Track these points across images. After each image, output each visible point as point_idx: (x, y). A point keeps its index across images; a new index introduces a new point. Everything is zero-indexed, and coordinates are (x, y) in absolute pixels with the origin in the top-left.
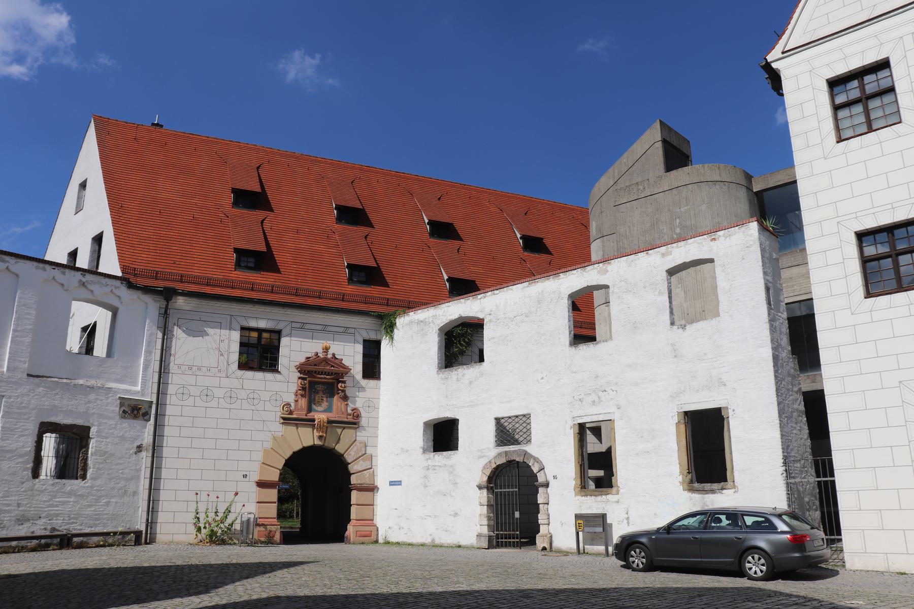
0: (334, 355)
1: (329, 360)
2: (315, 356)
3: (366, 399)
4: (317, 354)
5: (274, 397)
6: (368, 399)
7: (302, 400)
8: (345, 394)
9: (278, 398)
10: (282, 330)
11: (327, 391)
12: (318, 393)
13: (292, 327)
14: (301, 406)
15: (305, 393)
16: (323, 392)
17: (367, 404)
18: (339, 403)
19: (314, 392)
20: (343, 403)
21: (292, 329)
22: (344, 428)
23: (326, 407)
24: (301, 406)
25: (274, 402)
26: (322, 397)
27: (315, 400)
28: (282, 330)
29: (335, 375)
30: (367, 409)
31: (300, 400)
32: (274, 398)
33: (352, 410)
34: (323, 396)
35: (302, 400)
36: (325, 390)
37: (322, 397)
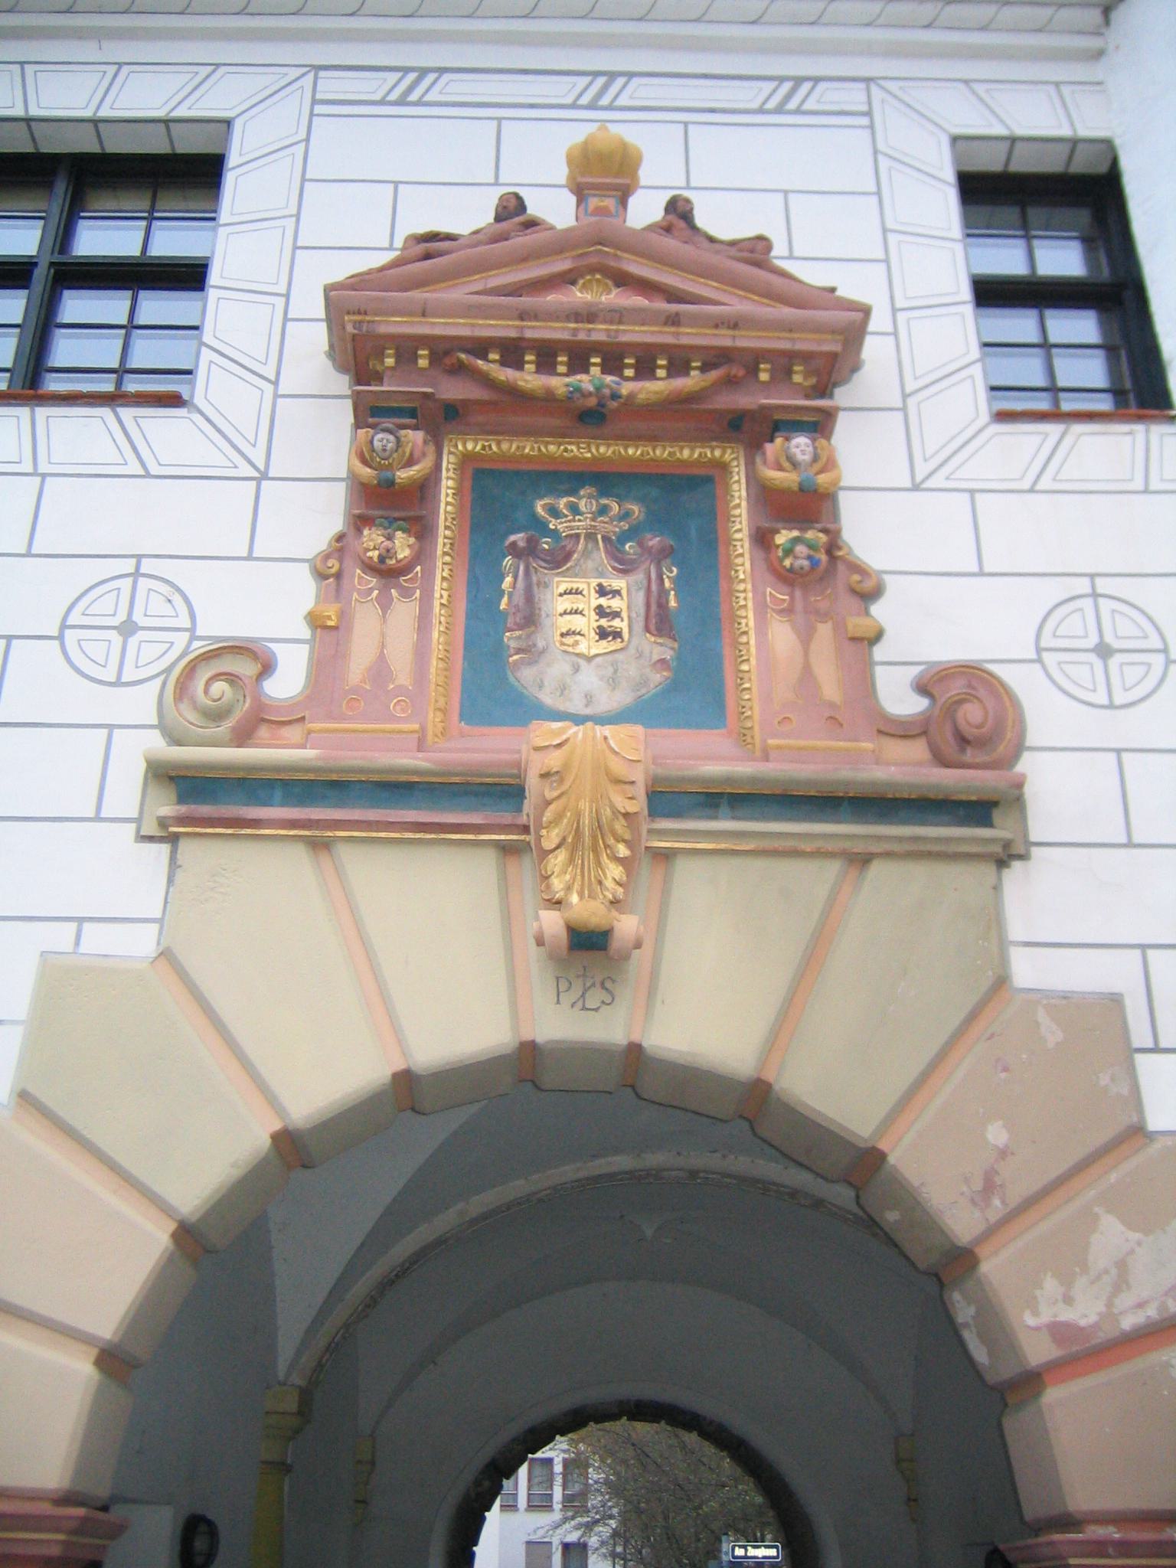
0: (679, 211)
1: (635, 245)
2: (498, 219)
3: (1057, 590)
4: (512, 209)
5: (106, 605)
6: (1083, 586)
7: (385, 604)
8: (833, 546)
9: (152, 607)
10: (228, 123)
11: (654, 542)
12: (559, 560)
13: (315, 102)
14: (380, 670)
15: (422, 555)
16: (614, 547)
17: (1078, 627)
18: (782, 635)
19: (530, 551)
20: (824, 630)
21: (318, 109)
22: (861, 861)
23: (657, 678)
24: (380, 670)
25: (102, 648)
26: (602, 591)
27: (530, 618)
28: (228, 123)
29: (714, 375)
30: (1085, 672)
31: (366, 622)
32: (108, 607)
33: (922, 688)
34: (619, 583)
35: (385, 604)
36: (632, 533)
37: (602, 591)
